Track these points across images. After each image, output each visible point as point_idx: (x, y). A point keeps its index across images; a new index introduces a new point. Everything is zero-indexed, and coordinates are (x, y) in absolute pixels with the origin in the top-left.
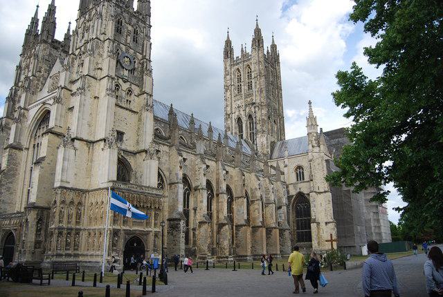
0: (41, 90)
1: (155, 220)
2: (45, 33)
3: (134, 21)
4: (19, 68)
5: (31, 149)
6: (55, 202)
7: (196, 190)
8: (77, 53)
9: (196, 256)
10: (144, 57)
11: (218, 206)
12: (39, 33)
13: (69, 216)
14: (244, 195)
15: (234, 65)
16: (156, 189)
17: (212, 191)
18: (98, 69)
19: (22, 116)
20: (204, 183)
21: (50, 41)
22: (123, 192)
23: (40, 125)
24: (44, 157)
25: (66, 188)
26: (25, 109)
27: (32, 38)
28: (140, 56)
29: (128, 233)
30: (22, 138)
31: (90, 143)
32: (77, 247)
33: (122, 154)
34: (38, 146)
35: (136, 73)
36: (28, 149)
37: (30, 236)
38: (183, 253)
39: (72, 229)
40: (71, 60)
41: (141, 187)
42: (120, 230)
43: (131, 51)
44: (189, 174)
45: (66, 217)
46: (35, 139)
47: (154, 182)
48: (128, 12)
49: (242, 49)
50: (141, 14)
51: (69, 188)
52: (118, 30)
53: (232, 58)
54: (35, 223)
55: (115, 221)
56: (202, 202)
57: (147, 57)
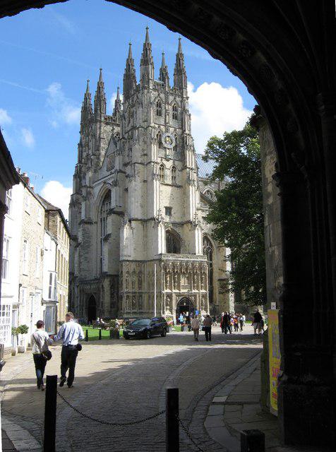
5: (99, 223)
8: (126, 136)
13: (133, 283)
18: (145, 155)
19: (89, 193)
24: (109, 235)
25: (128, 261)
26: (90, 187)
30: (91, 213)
32: (141, 306)
35: (178, 149)
37: (106, 299)
39: (135, 293)
40: (122, 145)
46: (101, 213)
54: (109, 288)
57: (187, 132)
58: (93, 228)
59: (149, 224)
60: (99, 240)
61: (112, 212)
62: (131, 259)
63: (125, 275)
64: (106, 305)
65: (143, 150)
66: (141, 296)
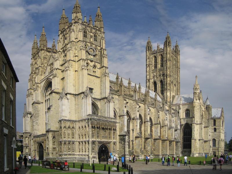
3: (94, 31)
5: (44, 102)
6: (61, 127)
7: (133, 119)
11: (145, 128)
13: (69, 134)
14: (159, 123)
16: (114, 119)
17: (142, 120)
20: (138, 116)
22: (96, 121)
25: (65, 120)
33: (93, 100)
34: (48, 101)
39: (70, 141)
41: (105, 118)
42: (96, 141)
43: (94, 46)
44: (129, 111)
46: (46, 97)
47: (112, 115)
50: (97, 27)
51: (67, 120)
54: (52, 139)
55: (93, 136)
56: (137, 126)
58: (40, 106)
64: (50, 149)
66: (73, 143)
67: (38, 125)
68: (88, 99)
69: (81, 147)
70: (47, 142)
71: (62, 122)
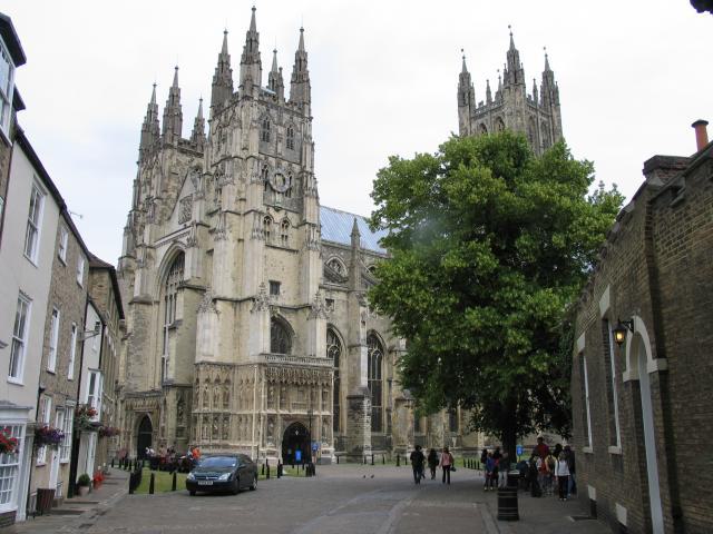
0: (169, 218)
1: (323, 400)
2: (169, 132)
3: (286, 117)
4: (137, 182)
6: (198, 380)
7: (390, 352)
9: (391, 449)
10: (302, 171)
12: (161, 126)
13: (215, 398)
15: (476, 118)
19: (149, 256)
21: (176, 143)
23: (172, 270)
25: (209, 363)
26: (150, 247)
27: (151, 140)
28: (297, 168)
29: (286, 418)
31: (236, 302)
32: (226, 435)
35: (292, 194)
36: (158, 303)
37: (169, 421)
38: (370, 445)
41: (303, 359)
43: (284, 164)
45: (211, 399)
47: (320, 346)
48: (277, 107)
49: (488, 87)
51: (214, 364)
52: (265, 138)
53: (471, 105)
55: (269, 404)
57: (308, 169)
58: (152, 311)
59: (244, 306)
60: (161, 329)
61: (183, 286)
62: (213, 360)
63: (203, 386)
65: (239, 192)
67: (142, 364)
68: (261, 317)
69: (242, 428)
70: (163, 412)
71: (201, 369)
